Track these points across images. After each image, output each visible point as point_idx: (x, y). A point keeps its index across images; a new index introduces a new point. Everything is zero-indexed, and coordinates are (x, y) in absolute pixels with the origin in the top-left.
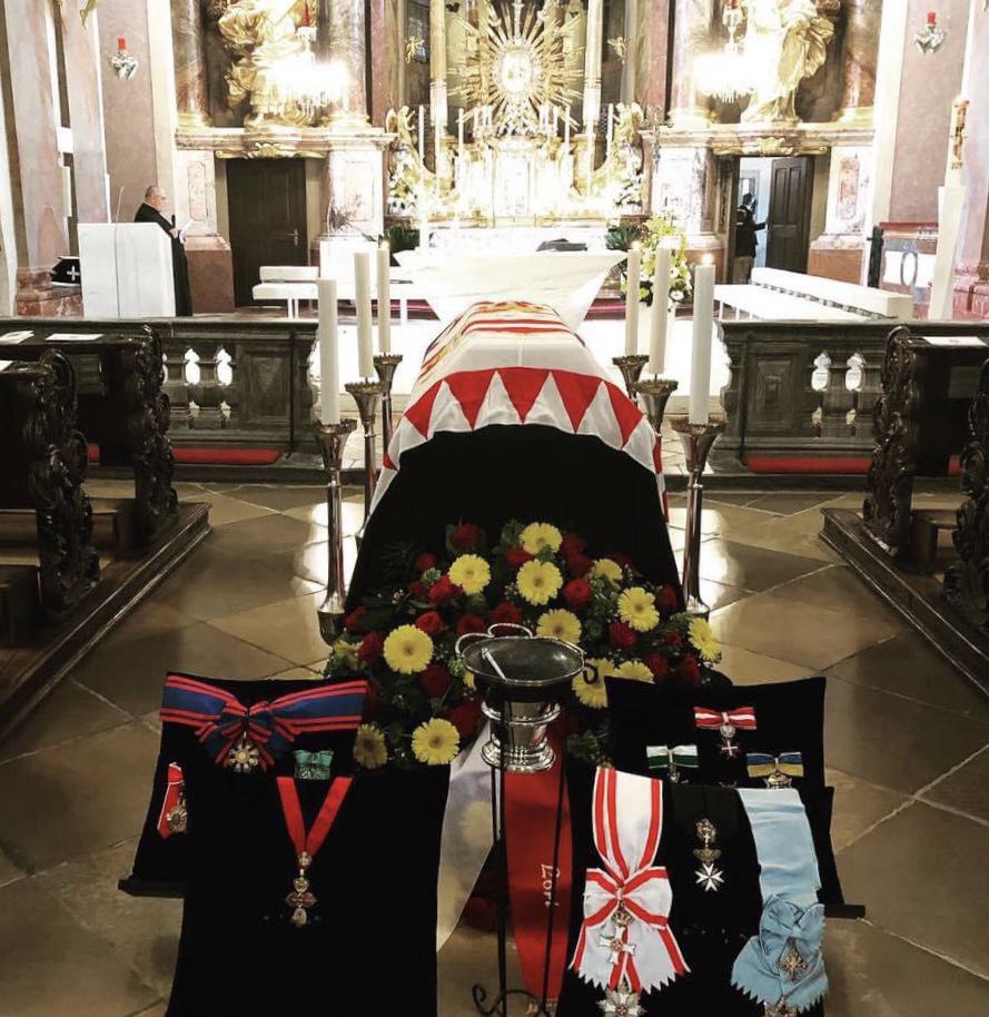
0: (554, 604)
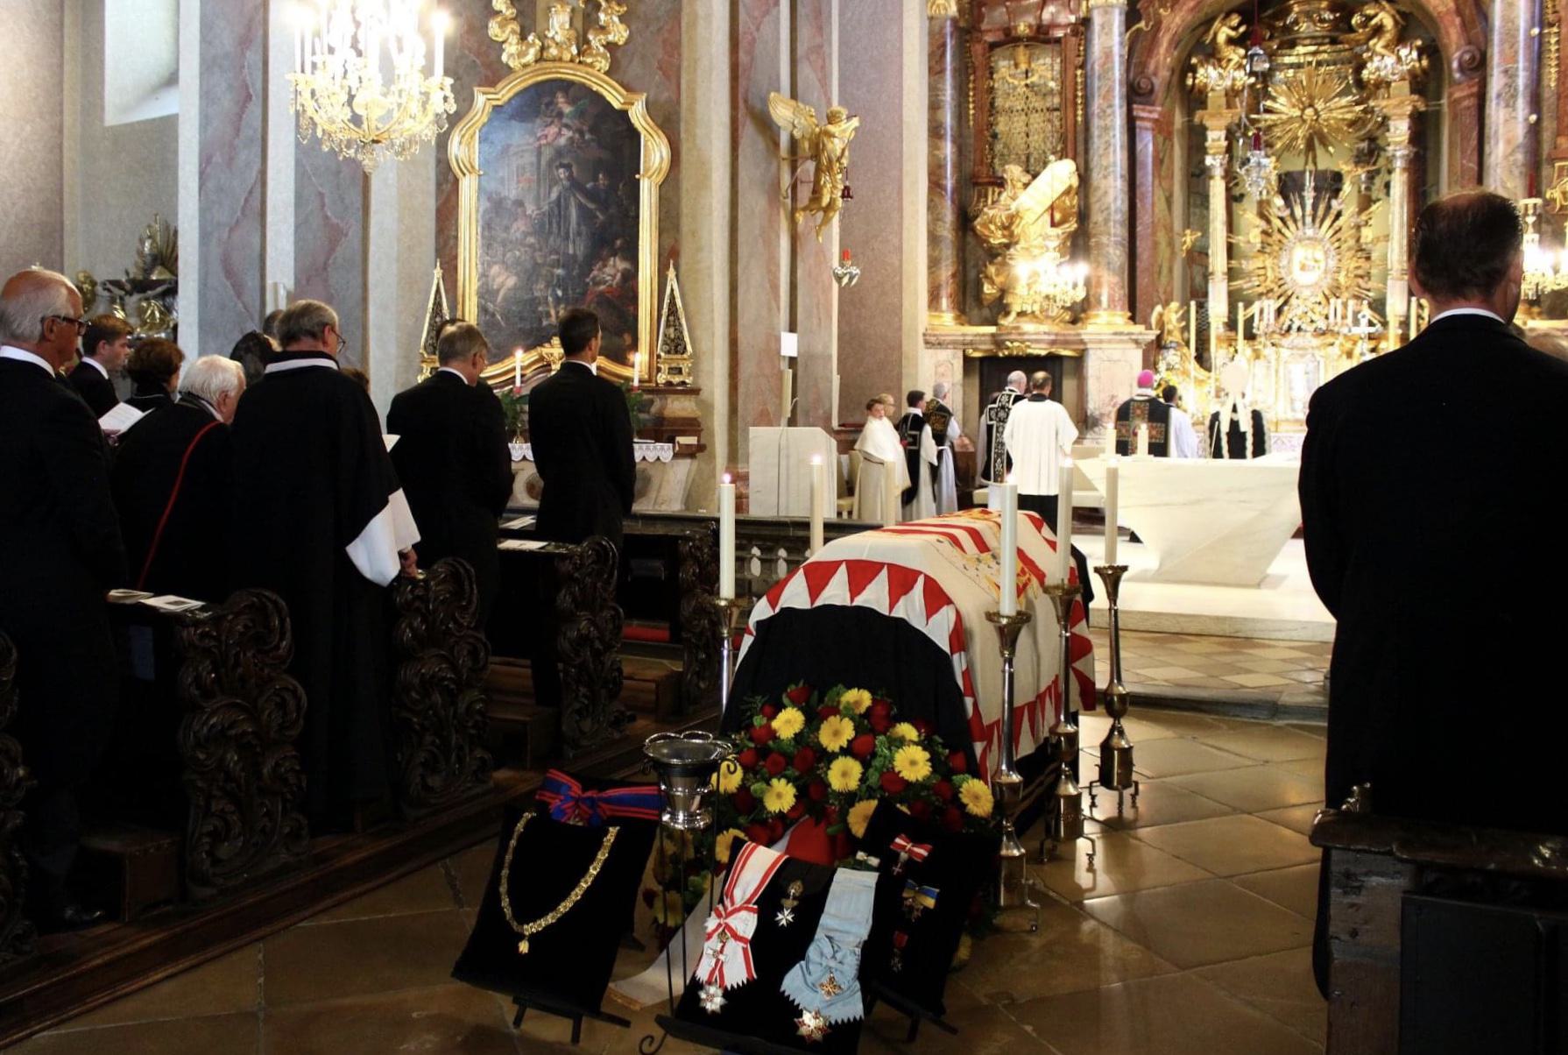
0: (845, 752)
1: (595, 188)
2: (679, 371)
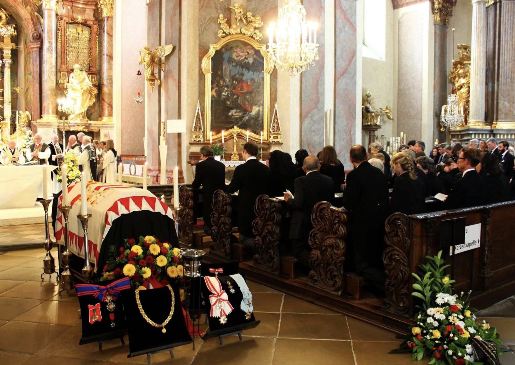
0: (160, 254)
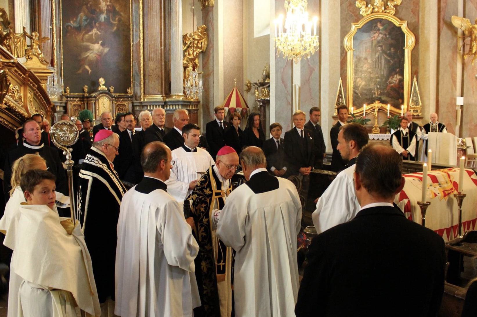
1: (390, 53)
2: (417, 111)
